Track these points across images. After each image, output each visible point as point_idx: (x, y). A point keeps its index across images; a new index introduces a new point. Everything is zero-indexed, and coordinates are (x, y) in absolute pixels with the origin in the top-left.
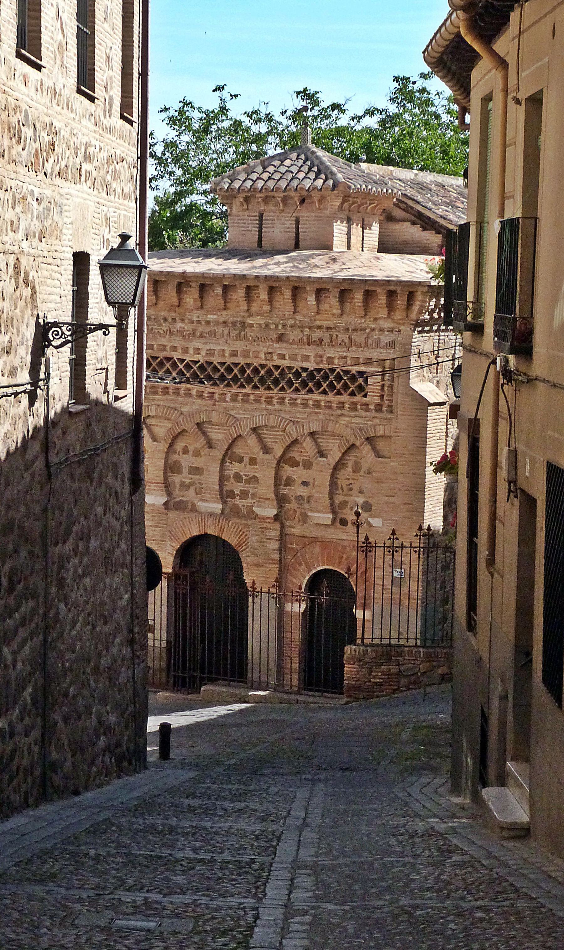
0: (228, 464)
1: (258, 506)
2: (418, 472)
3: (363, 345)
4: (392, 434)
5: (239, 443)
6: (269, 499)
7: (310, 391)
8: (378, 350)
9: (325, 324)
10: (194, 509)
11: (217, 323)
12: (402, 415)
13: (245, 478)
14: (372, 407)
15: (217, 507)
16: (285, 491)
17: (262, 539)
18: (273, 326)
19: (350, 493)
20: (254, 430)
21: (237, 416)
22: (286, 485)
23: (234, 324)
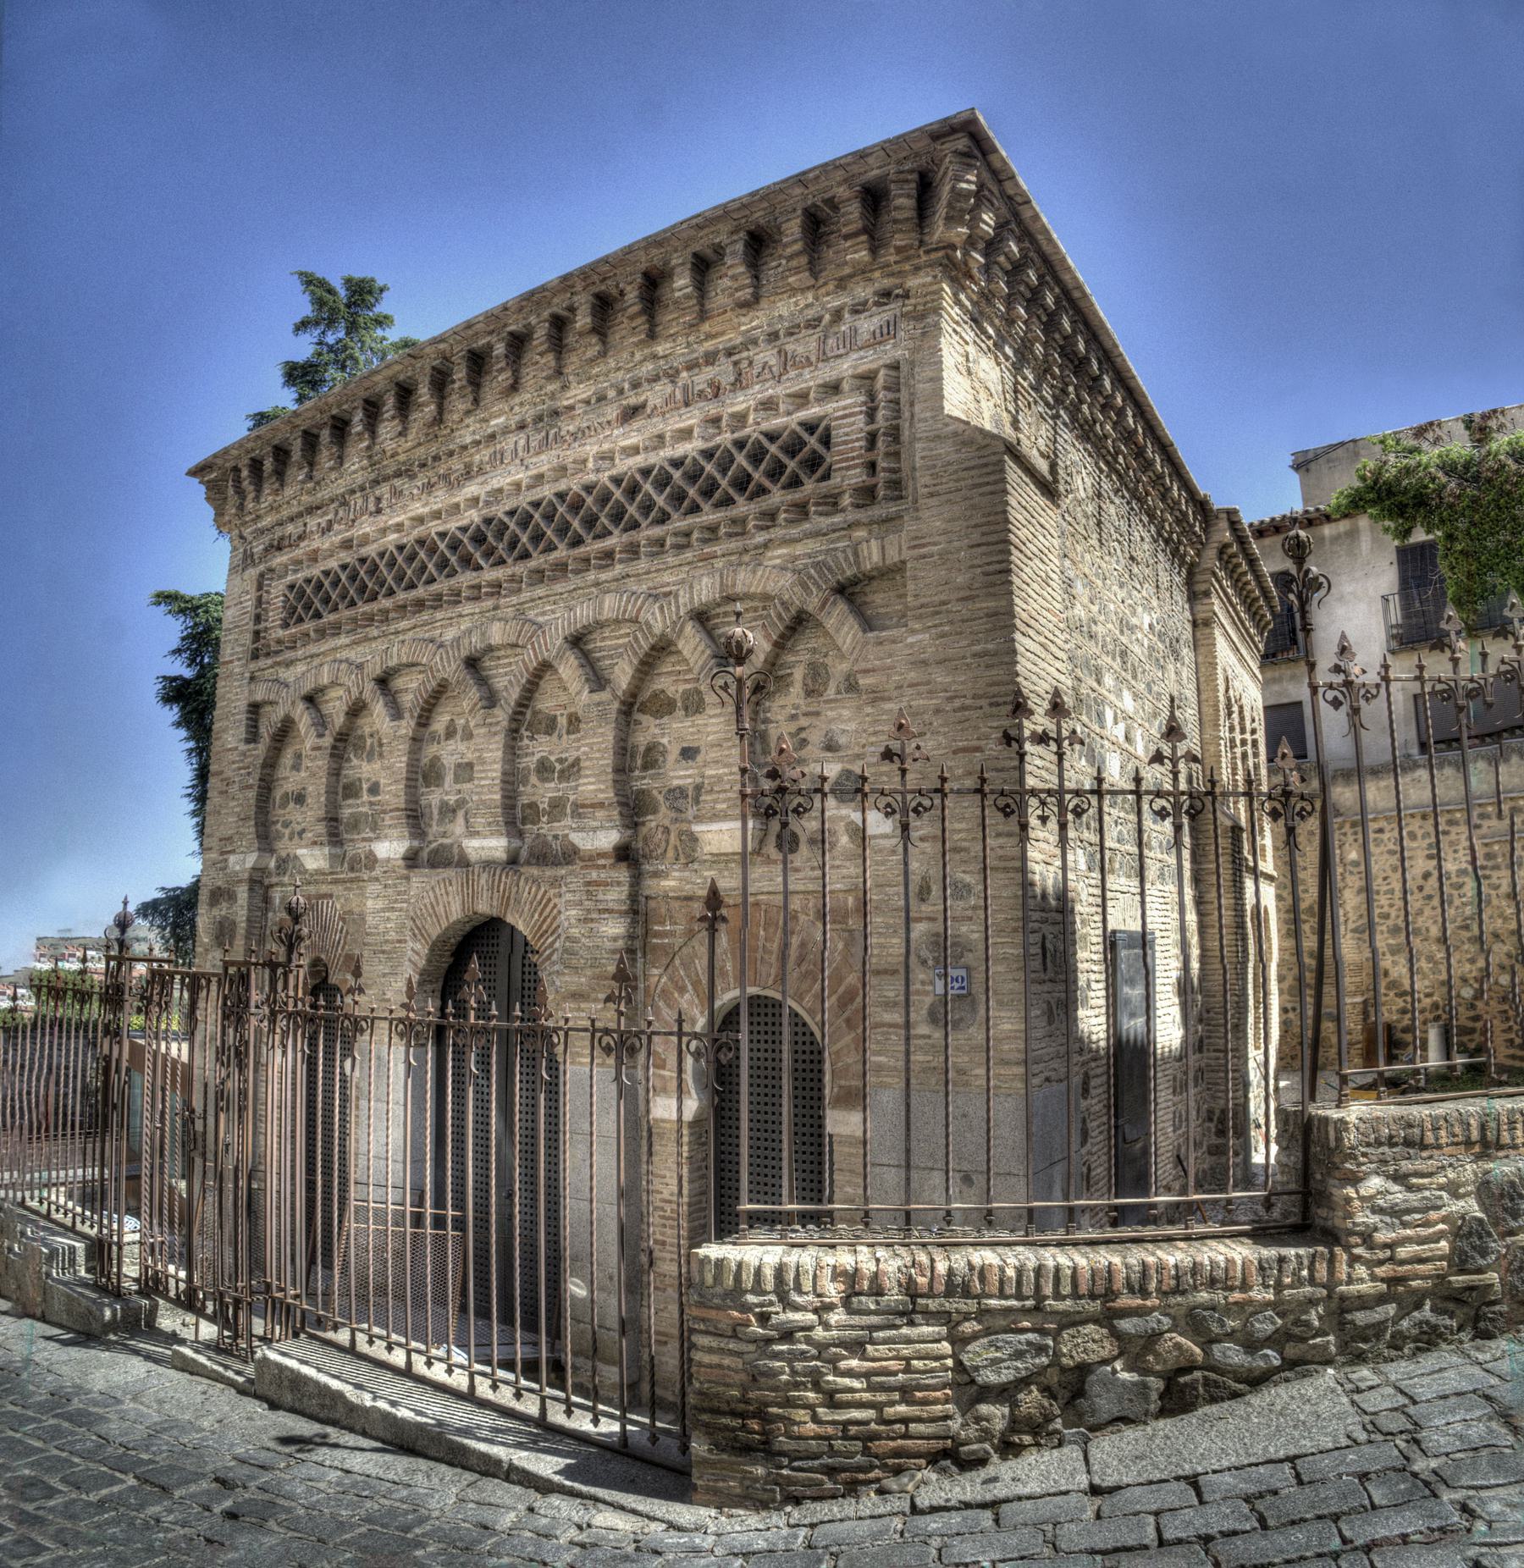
0: (526, 741)
1: (581, 829)
2: (990, 646)
3: (813, 359)
4: (907, 554)
5: (547, 684)
6: (601, 805)
7: (695, 509)
8: (855, 356)
9: (720, 343)
10: (464, 863)
11: (506, 431)
12: (932, 495)
13: (558, 767)
14: (846, 500)
15: (491, 845)
16: (642, 782)
17: (589, 911)
18: (611, 394)
19: (803, 753)
20: (577, 641)
21: (541, 619)
22: (645, 767)
23: (539, 418)
